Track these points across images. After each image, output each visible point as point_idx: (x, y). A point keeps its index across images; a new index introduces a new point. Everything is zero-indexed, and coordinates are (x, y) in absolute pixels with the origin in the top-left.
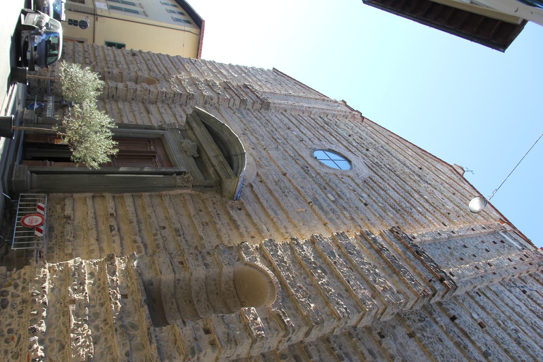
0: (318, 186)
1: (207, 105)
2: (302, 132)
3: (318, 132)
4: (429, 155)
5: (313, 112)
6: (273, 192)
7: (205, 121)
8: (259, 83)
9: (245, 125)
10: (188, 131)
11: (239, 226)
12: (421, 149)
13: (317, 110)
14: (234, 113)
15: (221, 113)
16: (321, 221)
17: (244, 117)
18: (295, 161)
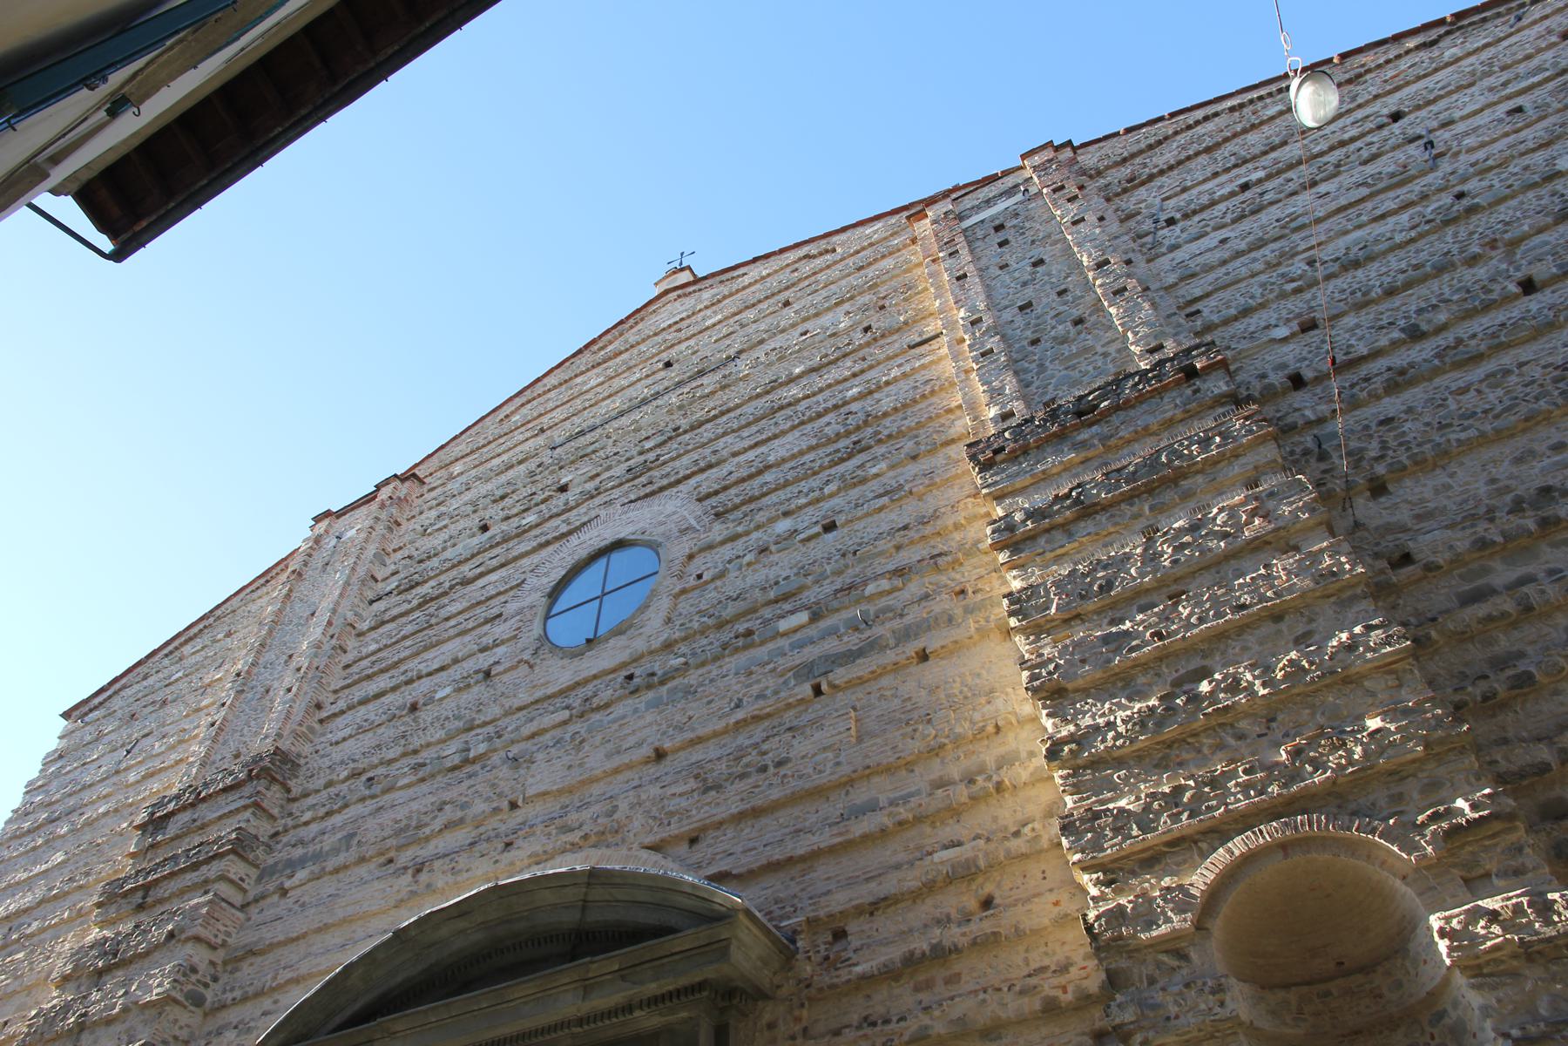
0: (731, 655)
1: (209, 995)
2: (442, 669)
3: (447, 619)
4: (609, 337)
5: (350, 616)
6: (758, 802)
7: (348, 1013)
8: (132, 777)
9: (362, 860)
11: (934, 948)
12: (580, 352)
13: (345, 603)
14: (284, 892)
15: (272, 947)
16: (906, 666)
17: (318, 857)
18: (593, 710)
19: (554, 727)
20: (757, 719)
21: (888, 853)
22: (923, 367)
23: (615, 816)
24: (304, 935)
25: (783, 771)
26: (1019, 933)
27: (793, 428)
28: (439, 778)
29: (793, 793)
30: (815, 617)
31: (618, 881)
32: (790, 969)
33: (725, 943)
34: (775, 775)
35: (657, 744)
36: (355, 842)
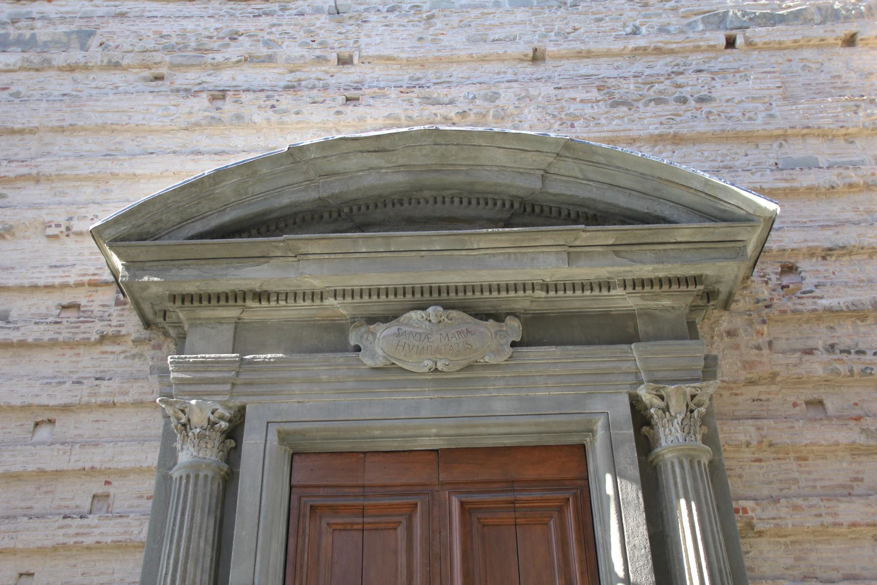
6: (683, 130)
7: (214, 222)
9: (116, 66)
10: (247, 316)
20: (658, 51)
21: (836, 209)
23: (497, 103)
24: (33, 131)
25: (706, 108)
29: (723, 131)
31: (596, 158)
32: (745, 288)
33: (740, 244)
34: (697, 109)
35: (536, 44)
36: (94, 42)
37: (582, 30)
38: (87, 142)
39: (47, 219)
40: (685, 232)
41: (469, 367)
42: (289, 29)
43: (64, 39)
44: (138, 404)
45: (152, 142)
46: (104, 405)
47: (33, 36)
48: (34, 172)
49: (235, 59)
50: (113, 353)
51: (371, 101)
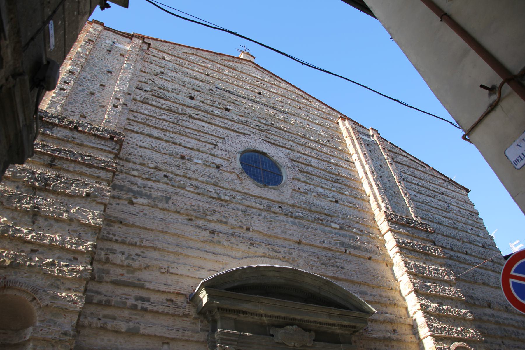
2: (192, 149)
3: (187, 127)
9: (178, 212)
17: (149, 197)
19: (256, 208)
20: (329, 249)
22: (351, 170)
24: (152, 230)
25: (343, 271)
26: (405, 341)
27: (316, 158)
28: (206, 198)
30: (341, 228)
35: (300, 239)
36: (170, 202)
37: (311, 237)
38: (170, 238)
39: (161, 265)
40: (356, 314)
41: (302, 346)
42: (231, 214)
43: (161, 198)
44: (197, 342)
45: (192, 244)
46: (187, 340)
47: (150, 194)
48: (155, 246)
49: (216, 220)
50: (186, 321)
51: (258, 246)
